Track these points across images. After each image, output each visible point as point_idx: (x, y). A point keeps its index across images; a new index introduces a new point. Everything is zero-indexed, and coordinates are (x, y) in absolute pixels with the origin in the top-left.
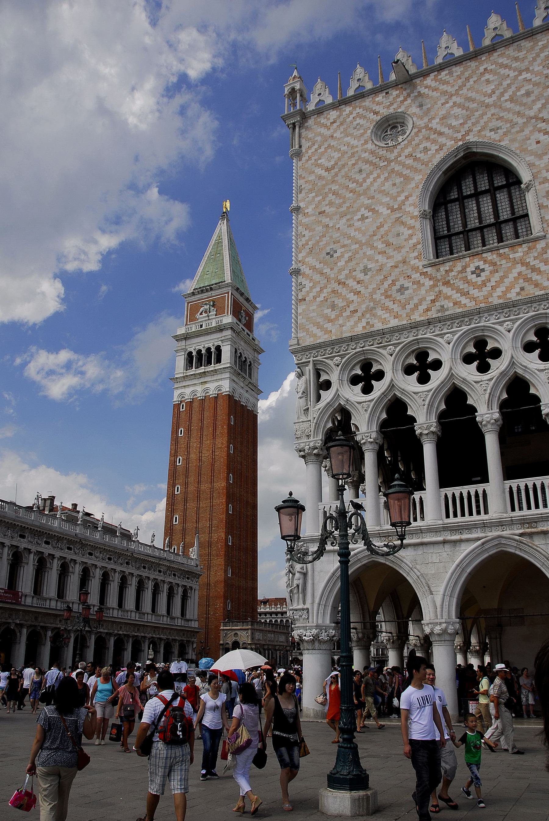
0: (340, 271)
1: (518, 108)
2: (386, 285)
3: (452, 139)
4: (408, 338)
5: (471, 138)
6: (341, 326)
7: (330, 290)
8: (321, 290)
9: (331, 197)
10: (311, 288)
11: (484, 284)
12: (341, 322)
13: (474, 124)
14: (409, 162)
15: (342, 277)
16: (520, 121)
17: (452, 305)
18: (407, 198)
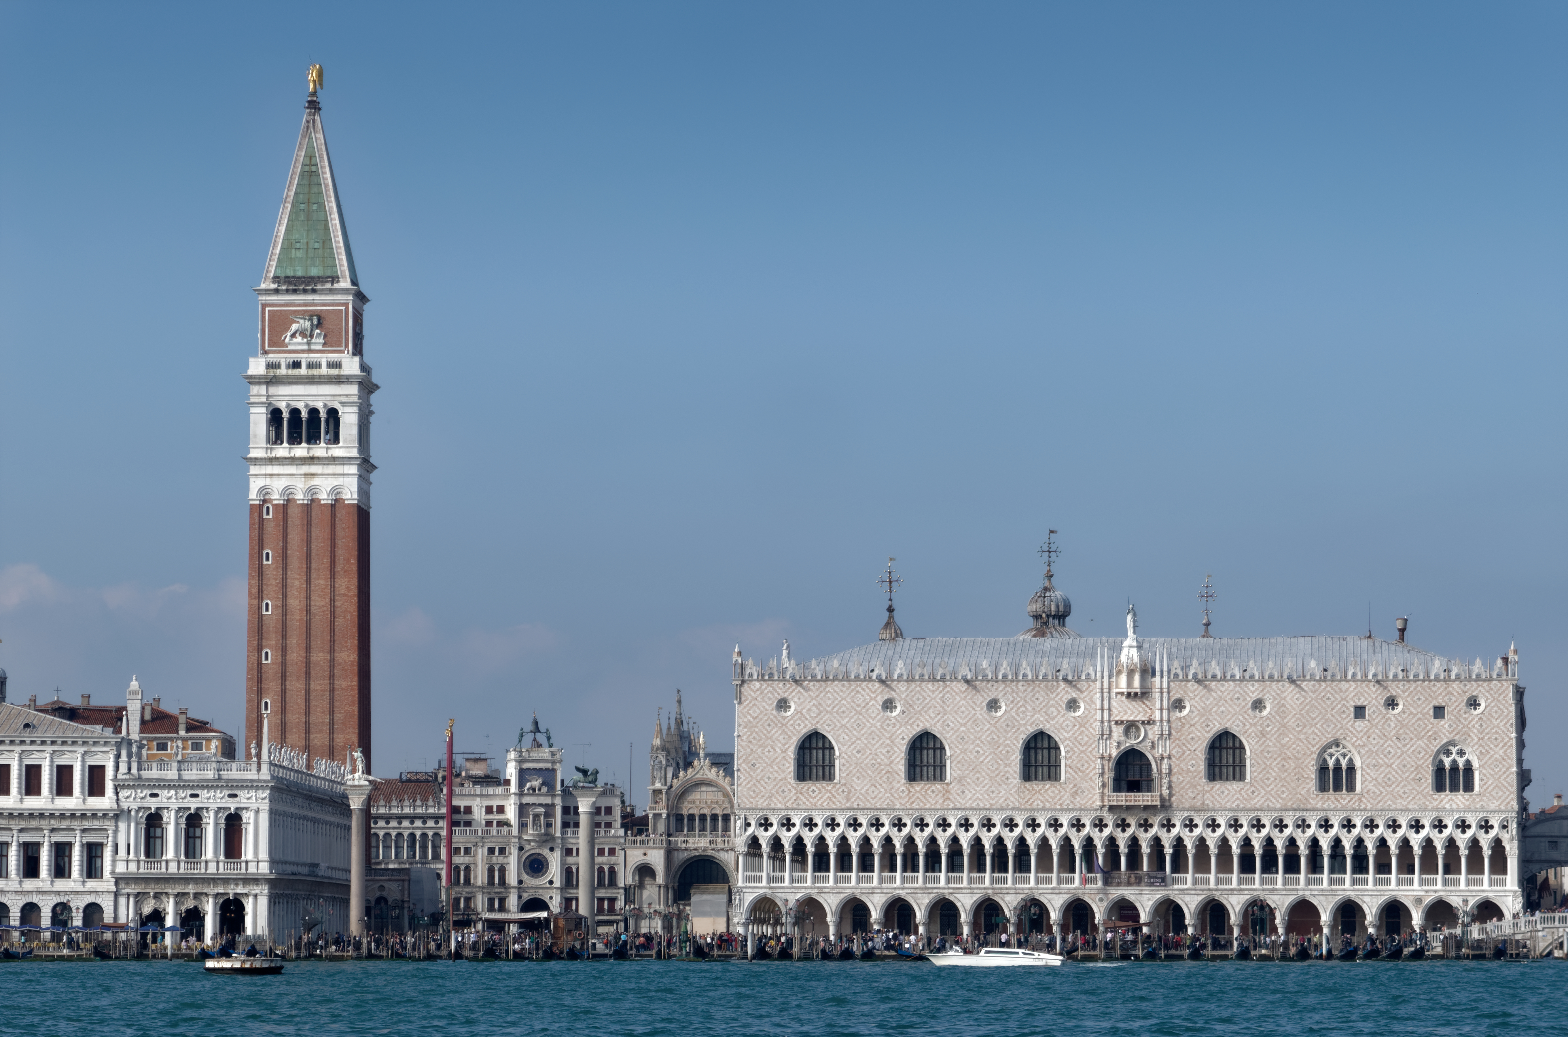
0: (758, 775)
5: (818, 726)
9: (754, 734)
14: (791, 728)
15: (758, 778)
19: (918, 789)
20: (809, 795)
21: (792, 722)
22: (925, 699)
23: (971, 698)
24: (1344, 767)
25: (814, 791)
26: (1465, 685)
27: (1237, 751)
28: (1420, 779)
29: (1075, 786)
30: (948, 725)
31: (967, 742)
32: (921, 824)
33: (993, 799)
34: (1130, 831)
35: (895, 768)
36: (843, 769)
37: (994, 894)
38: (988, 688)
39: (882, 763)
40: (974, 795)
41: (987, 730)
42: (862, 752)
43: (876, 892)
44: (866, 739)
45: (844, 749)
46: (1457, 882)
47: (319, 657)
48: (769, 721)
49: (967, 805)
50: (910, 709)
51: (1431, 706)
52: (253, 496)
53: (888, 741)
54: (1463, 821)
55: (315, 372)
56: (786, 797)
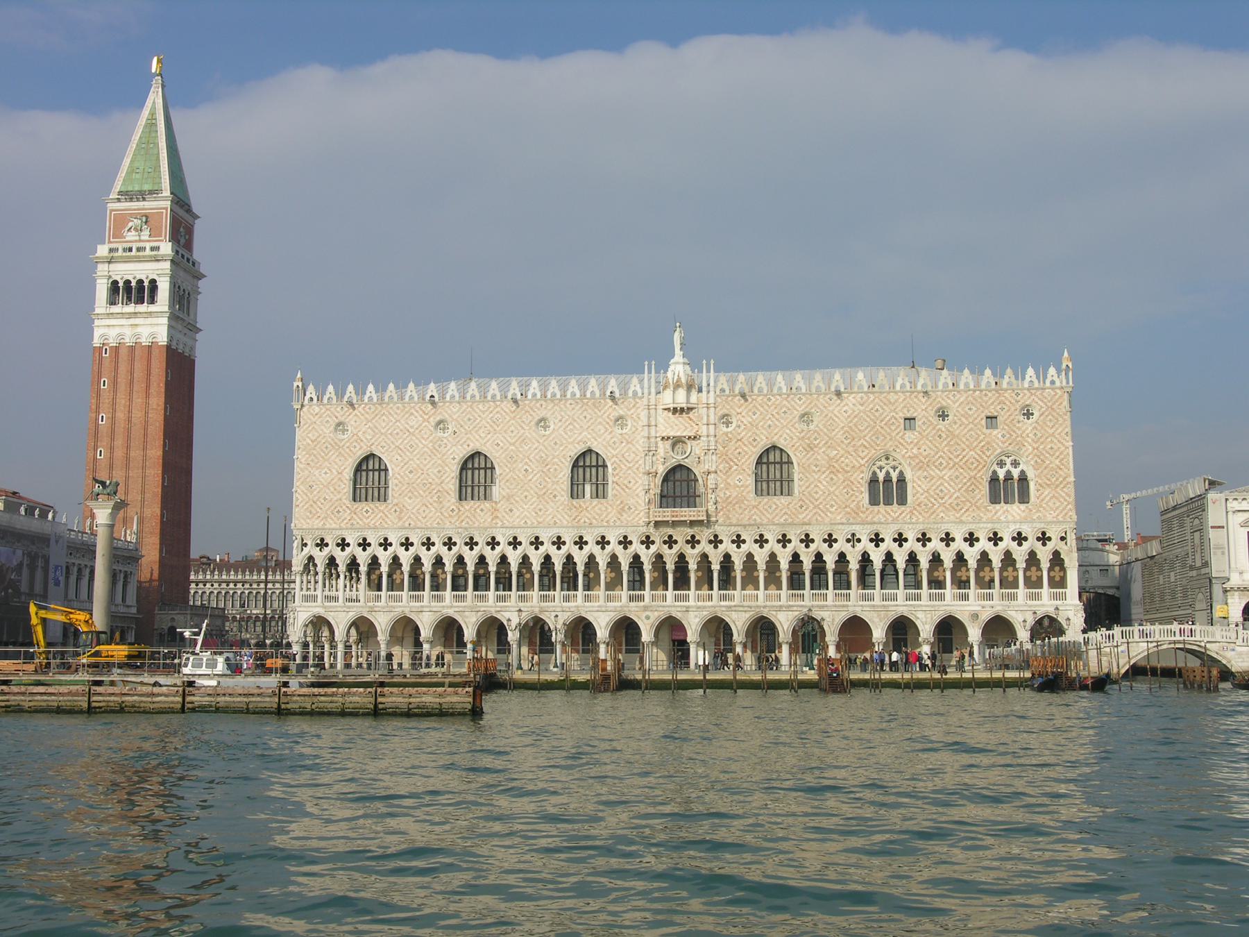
4: (338, 533)
24: (895, 480)
25: (367, 511)
26: (1017, 394)
27: (785, 466)
28: (973, 491)
30: (498, 445)
32: (471, 543)
34: (676, 548)
37: (541, 612)
43: (427, 611)
45: (397, 469)
46: (1013, 597)
47: (135, 453)
51: (983, 415)
52: (97, 342)
54: (1019, 534)
55: (141, 254)
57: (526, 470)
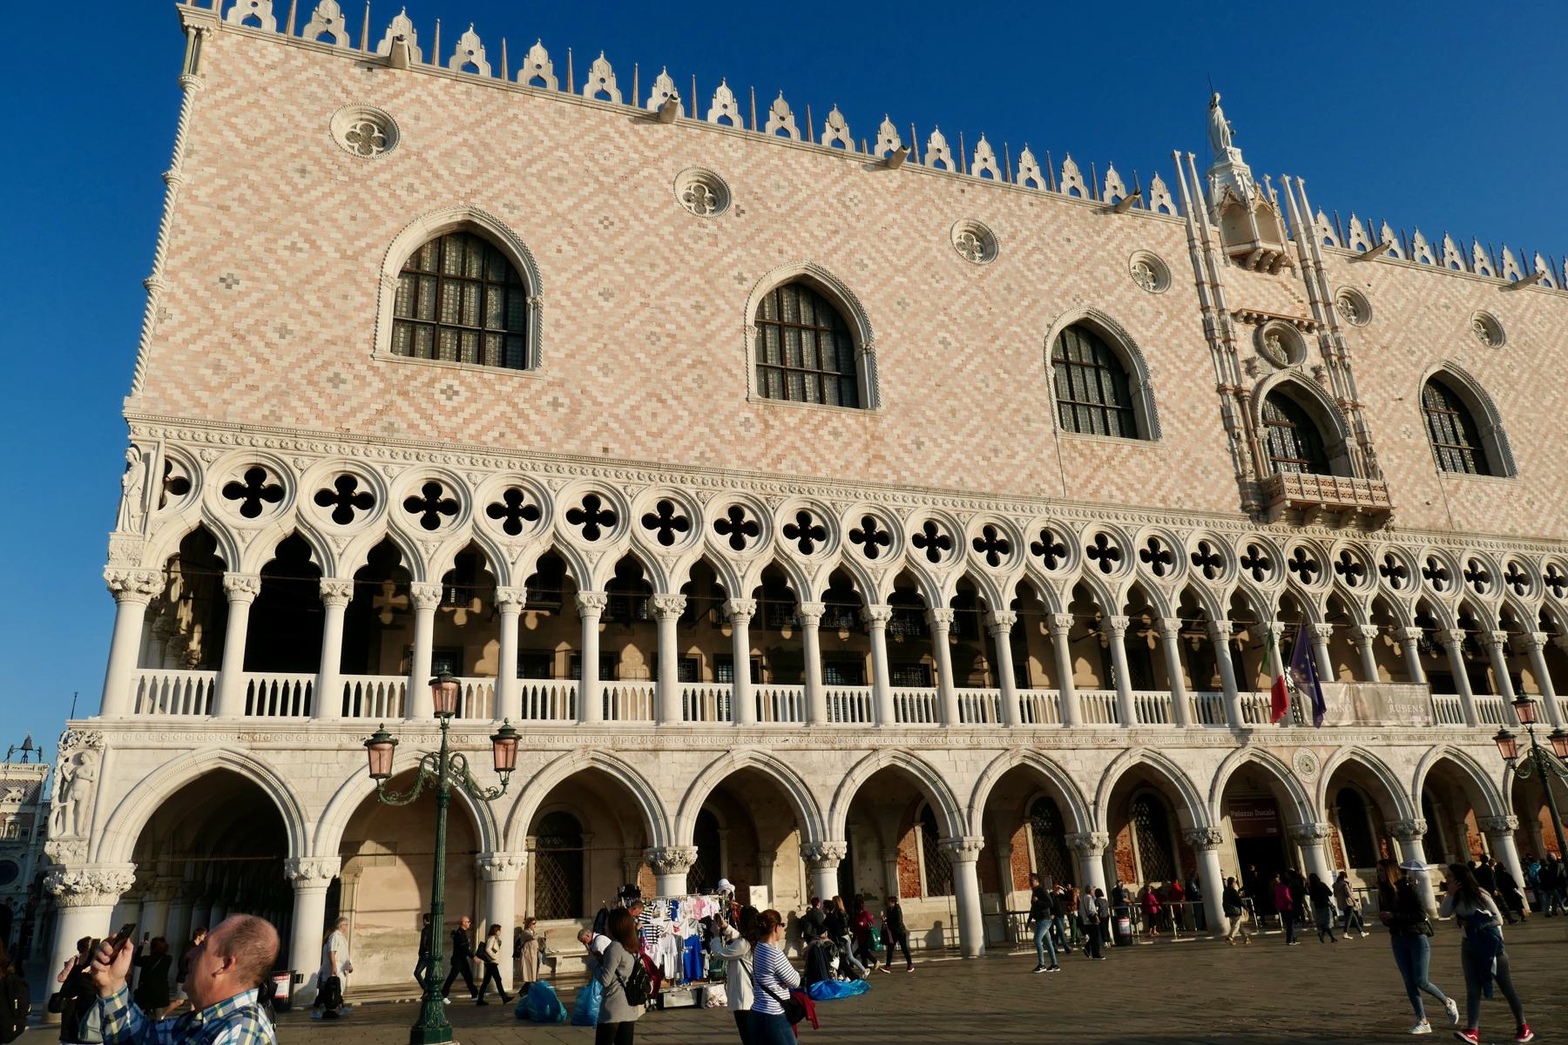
0: (239, 316)
1: (544, 193)
2: (313, 364)
3: (451, 190)
5: (478, 203)
6: (226, 402)
7: (216, 339)
8: (201, 334)
9: (243, 188)
10: (183, 325)
11: (455, 411)
12: (227, 395)
13: (485, 185)
15: (241, 326)
16: (545, 212)
17: (405, 426)
18: (370, 247)
19: (792, 421)
20: (436, 404)
21: (385, 176)
22: (796, 190)
23: (914, 211)
29: (1186, 454)
31: (915, 314)
33: (999, 471)
35: (721, 356)
36: (557, 337)
38: (951, 196)
39: (680, 335)
40: (949, 454)
41: (963, 292)
42: (619, 296)
44: (631, 262)
48: (304, 160)
49: (934, 482)
50: (756, 205)
53: (696, 280)
56: (343, 399)
57: (944, 342)
